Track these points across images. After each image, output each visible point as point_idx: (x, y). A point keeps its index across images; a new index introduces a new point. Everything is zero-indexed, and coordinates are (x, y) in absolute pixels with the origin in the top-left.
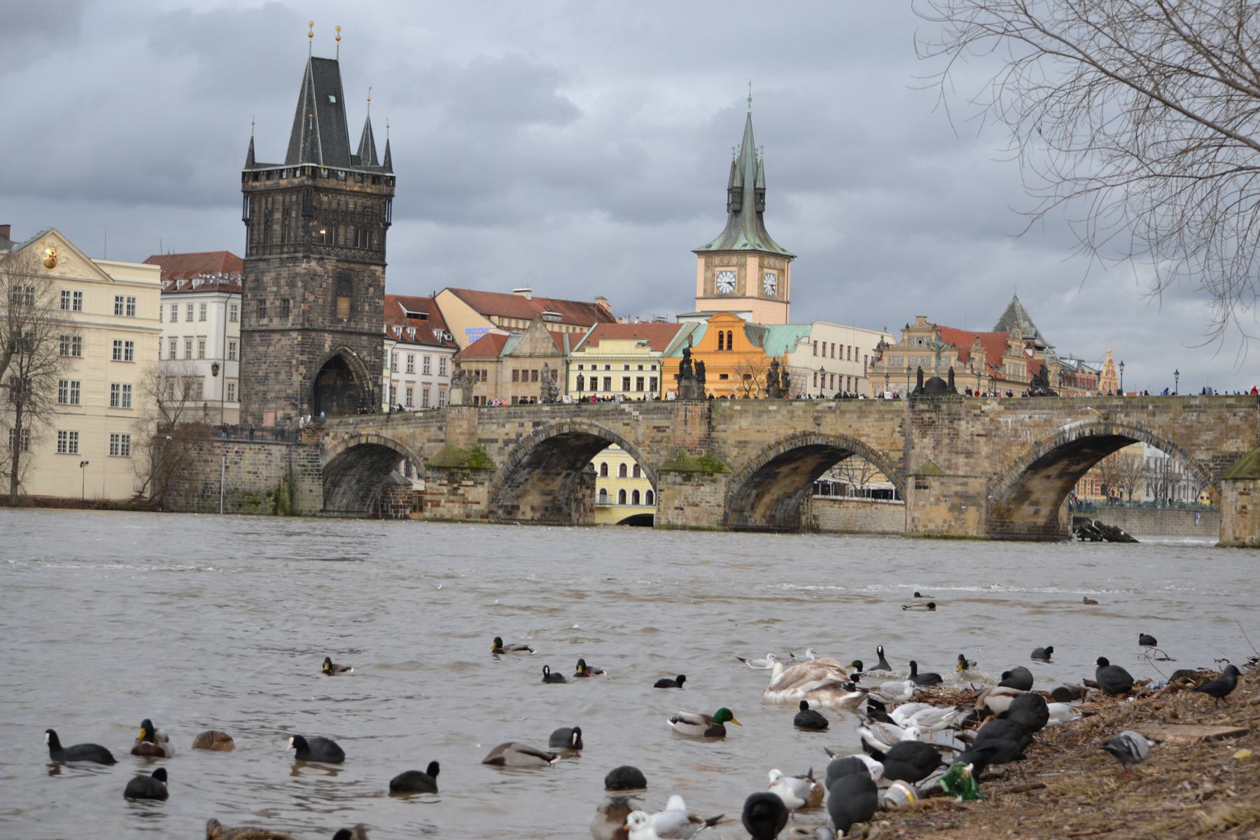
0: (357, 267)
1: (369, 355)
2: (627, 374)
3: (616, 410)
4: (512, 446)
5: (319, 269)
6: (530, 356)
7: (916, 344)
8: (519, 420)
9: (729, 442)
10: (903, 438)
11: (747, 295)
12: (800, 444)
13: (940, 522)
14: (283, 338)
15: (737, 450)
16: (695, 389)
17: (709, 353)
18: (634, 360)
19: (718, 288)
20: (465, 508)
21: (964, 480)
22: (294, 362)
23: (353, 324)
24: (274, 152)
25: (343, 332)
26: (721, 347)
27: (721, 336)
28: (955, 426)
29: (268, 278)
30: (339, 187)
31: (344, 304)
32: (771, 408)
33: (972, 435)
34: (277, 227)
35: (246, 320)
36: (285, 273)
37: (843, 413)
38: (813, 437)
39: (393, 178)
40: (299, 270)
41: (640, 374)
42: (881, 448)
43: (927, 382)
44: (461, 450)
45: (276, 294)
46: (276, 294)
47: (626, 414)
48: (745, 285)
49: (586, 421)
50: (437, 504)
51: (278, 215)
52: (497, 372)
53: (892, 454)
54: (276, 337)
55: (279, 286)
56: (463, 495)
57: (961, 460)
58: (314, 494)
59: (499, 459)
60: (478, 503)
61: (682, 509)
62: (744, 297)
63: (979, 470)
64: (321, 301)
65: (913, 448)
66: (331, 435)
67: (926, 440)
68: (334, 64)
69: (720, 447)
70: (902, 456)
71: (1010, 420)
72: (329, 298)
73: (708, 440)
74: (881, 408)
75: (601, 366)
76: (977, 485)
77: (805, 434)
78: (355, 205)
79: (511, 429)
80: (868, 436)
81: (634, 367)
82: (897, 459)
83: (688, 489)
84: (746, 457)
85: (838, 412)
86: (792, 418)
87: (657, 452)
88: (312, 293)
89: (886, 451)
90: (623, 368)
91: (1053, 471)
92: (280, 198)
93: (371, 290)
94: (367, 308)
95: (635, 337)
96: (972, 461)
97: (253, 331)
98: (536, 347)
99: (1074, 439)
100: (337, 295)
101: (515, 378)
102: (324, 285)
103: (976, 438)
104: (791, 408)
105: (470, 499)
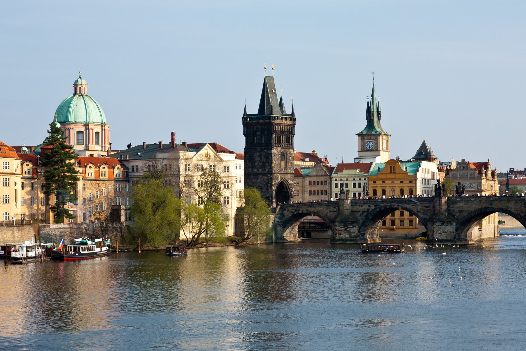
0: (286, 150)
2: (354, 182)
3: (409, 200)
4: (366, 213)
5: (276, 152)
6: (316, 176)
7: (462, 168)
8: (368, 204)
11: (378, 150)
12: (484, 211)
17: (387, 174)
18: (357, 177)
19: (366, 147)
20: (350, 235)
22: (269, 185)
23: (286, 171)
24: (254, 110)
25: (283, 173)
27: (391, 167)
29: (256, 155)
30: (281, 123)
31: (283, 163)
32: (472, 199)
36: (263, 153)
37: (501, 201)
38: (489, 209)
39: (295, 118)
40: (269, 152)
41: (360, 182)
45: (260, 161)
46: (260, 161)
48: (377, 146)
50: (340, 234)
52: (303, 182)
53: (521, 214)
54: (261, 176)
56: (349, 230)
59: (361, 218)
61: (441, 234)
64: (277, 163)
66: (287, 210)
73: (449, 211)
74: (516, 199)
75: (344, 179)
77: (486, 208)
78: (285, 128)
79: (365, 207)
80: (511, 208)
81: (357, 179)
82: (523, 216)
83: (443, 227)
85: (499, 200)
86: (480, 203)
87: (426, 214)
88: (275, 160)
93: (290, 158)
94: (289, 165)
98: (318, 173)
100: (281, 160)
101: (310, 184)
102: (278, 157)
104: (480, 199)
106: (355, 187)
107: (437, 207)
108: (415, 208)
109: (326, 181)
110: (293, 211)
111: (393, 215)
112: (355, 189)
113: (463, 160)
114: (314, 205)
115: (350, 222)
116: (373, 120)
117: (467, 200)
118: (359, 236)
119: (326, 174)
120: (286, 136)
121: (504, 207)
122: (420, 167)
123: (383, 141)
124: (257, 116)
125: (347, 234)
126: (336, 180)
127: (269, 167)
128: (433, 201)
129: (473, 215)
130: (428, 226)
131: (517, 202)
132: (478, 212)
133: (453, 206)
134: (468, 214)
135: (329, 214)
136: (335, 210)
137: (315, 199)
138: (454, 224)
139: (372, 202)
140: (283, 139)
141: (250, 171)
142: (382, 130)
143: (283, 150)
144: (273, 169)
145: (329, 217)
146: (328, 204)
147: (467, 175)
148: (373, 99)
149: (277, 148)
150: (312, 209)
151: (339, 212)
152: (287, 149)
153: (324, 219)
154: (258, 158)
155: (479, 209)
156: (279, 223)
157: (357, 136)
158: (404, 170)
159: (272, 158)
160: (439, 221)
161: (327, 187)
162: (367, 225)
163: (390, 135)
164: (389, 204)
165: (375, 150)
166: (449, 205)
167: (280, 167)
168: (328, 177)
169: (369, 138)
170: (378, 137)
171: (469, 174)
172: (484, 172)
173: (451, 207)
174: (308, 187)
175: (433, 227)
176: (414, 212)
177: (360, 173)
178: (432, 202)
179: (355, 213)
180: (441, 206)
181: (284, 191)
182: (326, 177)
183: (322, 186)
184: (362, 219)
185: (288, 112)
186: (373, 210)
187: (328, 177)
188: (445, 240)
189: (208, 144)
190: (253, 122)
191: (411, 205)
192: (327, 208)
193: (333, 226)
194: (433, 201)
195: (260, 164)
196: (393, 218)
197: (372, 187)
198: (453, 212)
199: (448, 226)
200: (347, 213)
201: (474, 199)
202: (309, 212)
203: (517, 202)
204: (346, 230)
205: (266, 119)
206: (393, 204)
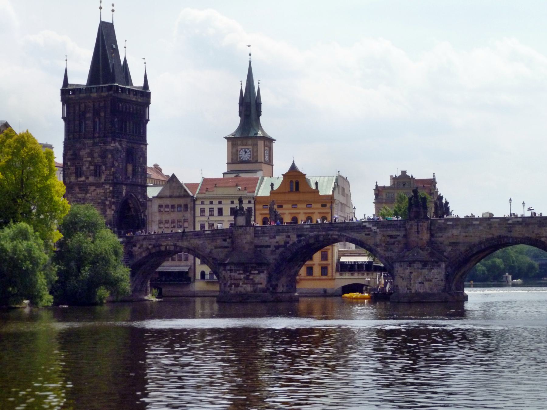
0: (135, 146)
1: (141, 198)
4: (281, 250)
5: (119, 147)
6: (171, 197)
7: (402, 186)
8: (286, 234)
14: (97, 189)
17: (285, 193)
19: (240, 158)
22: (107, 203)
26: (291, 191)
29: (83, 153)
31: (130, 168)
34: (89, 122)
35: (67, 179)
36: (97, 150)
39: (150, 93)
40: (108, 147)
45: (90, 162)
46: (90, 162)
47: (368, 228)
48: (257, 155)
50: (237, 286)
51: (89, 115)
54: (93, 188)
56: (252, 279)
59: (271, 258)
61: (423, 283)
62: (257, 162)
64: (121, 166)
66: (138, 246)
68: (112, 25)
69: (438, 246)
72: (124, 164)
75: (216, 202)
79: (280, 239)
83: (425, 271)
86: (490, 228)
88: (117, 161)
90: (230, 203)
92: (91, 105)
94: (140, 170)
100: (128, 162)
102: (122, 156)
105: (256, 282)
109: (186, 206)
110: (150, 247)
113: (404, 173)
114: (187, 236)
115: (254, 265)
119: (185, 193)
121: (533, 236)
125: (249, 285)
126: (203, 203)
127: (108, 172)
129: (475, 250)
134: (468, 248)
135: (214, 251)
136: (225, 244)
138: (443, 265)
143: (130, 145)
145: (215, 257)
150: (184, 244)
151: (234, 248)
153: (206, 261)
154: (88, 157)
155: (487, 240)
157: (226, 140)
158: (314, 187)
160: (419, 261)
163: (275, 140)
164: (324, 233)
165: (254, 161)
166: (433, 233)
167: (126, 174)
173: (436, 237)
174: (157, 214)
176: (369, 245)
178: (402, 229)
180: (420, 235)
185: (137, 82)
186: (294, 243)
187: (189, 200)
191: (363, 234)
193: (224, 272)
197: (261, 214)
198: (440, 245)
199: (433, 269)
202: (178, 248)
204: (247, 278)
206: (331, 233)
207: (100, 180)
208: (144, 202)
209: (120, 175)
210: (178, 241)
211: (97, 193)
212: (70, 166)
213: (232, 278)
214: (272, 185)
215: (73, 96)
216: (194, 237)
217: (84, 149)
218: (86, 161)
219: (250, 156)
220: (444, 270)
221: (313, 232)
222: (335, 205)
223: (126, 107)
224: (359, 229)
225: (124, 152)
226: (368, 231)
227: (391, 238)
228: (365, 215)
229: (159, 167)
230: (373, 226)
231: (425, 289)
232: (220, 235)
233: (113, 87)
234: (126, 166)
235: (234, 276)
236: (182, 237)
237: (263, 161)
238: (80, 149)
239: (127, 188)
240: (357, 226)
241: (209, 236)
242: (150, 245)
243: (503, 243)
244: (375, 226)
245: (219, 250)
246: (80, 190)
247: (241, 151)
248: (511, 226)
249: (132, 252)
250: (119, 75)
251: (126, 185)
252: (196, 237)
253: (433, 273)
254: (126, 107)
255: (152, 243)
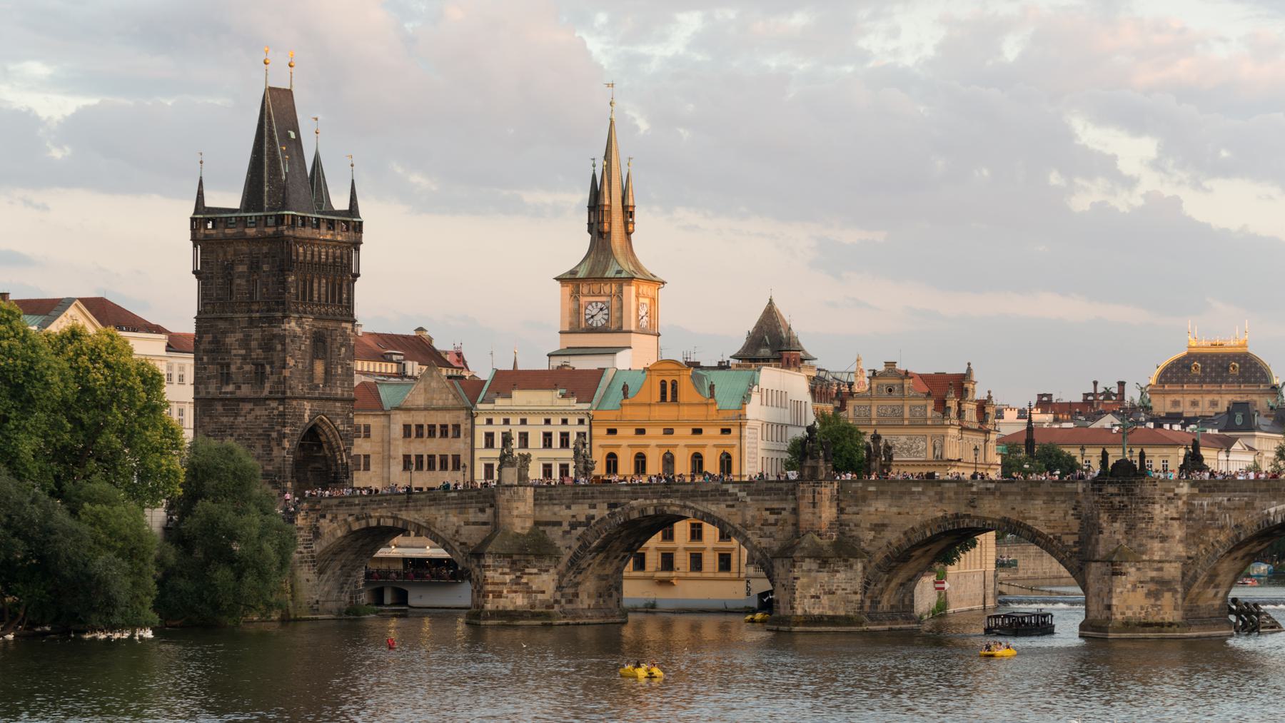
0: (331, 325)
2: (548, 429)
5: (298, 329)
6: (425, 409)
7: (885, 393)
8: (590, 501)
9: (862, 525)
10: (1079, 521)
11: (624, 329)
12: (951, 527)
13: (1136, 609)
14: (256, 408)
15: (873, 533)
16: (822, 468)
17: (650, 405)
18: (557, 413)
21: (1160, 565)
22: (274, 435)
24: (227, 197)
25: (320, 399)
26: (663, 398)
27: (663, 384)
28: (1149, 510)
29: (231, 339)
30: (313, 236)
31: (319, 367)
32: (914, 489)
33: (1166, 518)
36: (256, 334)
38: (967, 520)
39: (361, 223)
40: (276, 331)
41: (565, 429)
42: (1052, 531)
43: (1114, 465)
44: (518, 533)
45: (244, 358)
46: (244, 358)
47: (731, 495)
49: (677, 502)
50: (499, 595)
53: (1064, 538)
54: (248, 406)
55: (247, 347)
56: (527, 584)
57: (1156, 545)
58: (311, 583)
59: (565, 544)
60: (543, 592)
61: (818, 597)
62: (620, 330)
63: (1173, 554)
64: (300, 366)
65: (1101, 532)
66: (329, 516)
67: (1117, 525)
68: (288, 93)
69: (850, 530)
70: (1077, 540)
71: (1205, 503)
72: (308, 361)
73: (839, 524)
75: (515, 420)
76: (1172, 570)
77: (957, 516)
78: (327, 255)
79: (581, 511)
80: (1035, 518)
81: (556, 420)
82: (1071, 543)
83: (824, 576)
84: (885, 542)
85: (998, 494)
87: (771, 536)
88: (293, 357)
89: (1058, 535)
90: (543, 422)
91: (1240, 553)
93: (343, 350)
94: (339, 371)
95: (554, 387)
96: (1167, 545)
97: (213, 399)
98: (433, 398)
99: (1279, 522)
100: (315, 357)
103: (1170, 522)
104: (939, 489)
105: (534, 588)
106: (550, 446)
107: (806, 515)
108: (736, 514)
109: (457, 427)
111: (669, 536)
112: (548, 453)
114: (416, 500)
116: (609, 233)
117: (901, 493)
118: (557, 602)
120: (330, 280)
121: (1013, 516)
122: (754, 385)
123: (641, 300)
124: (236, 215)
125: (521, 595)
127: (274, 378)
128: (794, 494)
129: (917, 538)
130: (776, 571)
131: (1053, 500)
132: (931, 532)
133: (855, 509)
135: (465, 530)
136: (482, 517)
137: (424, 479)
138: (859, 566)
139: (600, 492)
140: (320, 287)
141: (212, 388)
142: (636, 264)
143: (320, 324)
144: (287, 385)
145: (463, 540)
146: (462, 498)
147: (903, 412)
148: (608, 168)
149: (301, 318)
150: (409, 515)
152: (333, 320)
153: (448, 547)
154: (241, 347)
156: (303, 557)
157: (558, 282)
159: (284, 350)
160: (810, 557)
161: (456, 446)
162: (585, 565)
163: (663, 283)
164: (655, 501)
166: (842, 505)
167: (311, 378)
168: (465, 412)
169: (597, 291)
170: (625, 288)
171: (907, 410)
172: (952, 404)
175: (791, 575)
176: (733, 527)
177: (565, 402)
178: (791, 497)
179: (548, 529)
180: (817, 510)
181: (321, 454)
182: (456, 413)
183: (445, 442)
184: (570, 548)
185: (340, 202)
186: (602, 519)
188: (828, 616)
189: (77, 302)
190: (224, 233)
191: (723, 506)
192: (458, 511)
193: (477, 570)
194: (793, 491)
195: (247, 368)
196: (667, 545)
197: (601, 446)
199: (838, 571)
200: (522, 528)
201: (920, 489)
203: (1053, 500)
204: (516, 581)
205: (266, 225)
206: (669, 501)
207: (262, 392)
208: (347, 431)
209: (299, 382)
210: (400, 510)
211: (257, 416)
212: (208, 363)
213: (489, 581)
214: (625, 388)
215: (213, 232)
216: (428, 503)
217: (232, 332)
218: (235, 355)
219: (606, 317)
220: (861, 574)
221: (636, 499)
222: (747, 431)
223: (312, 255)
224: (715, 495)
225: (308, 338)
226: (732, 500)
227: (771, 514)
228: (1095, 383)
229: (427, 333)
230: (740, 491)
231: (823, 608)
232: (474, 501)
233: (286, 217)
234: (312, 364)
235: (493, 577)
236: (408, 502)
237: (633, 328)
238: (225, 333)
239: (312, 406)
240: (712, 491)
241: (455, 502)
242: (350, 515)
243: (962, 526)
244: (745, 491)
245: (473, 527)
246: (224, 409)
247: (590, 307)
248: (975, 496)
249: (318, 528)
250: (299, 192)
251: (310, 399)
252: (432, 503)
253: (838, 579)
254: (312, 255)
255: (353, 512)
